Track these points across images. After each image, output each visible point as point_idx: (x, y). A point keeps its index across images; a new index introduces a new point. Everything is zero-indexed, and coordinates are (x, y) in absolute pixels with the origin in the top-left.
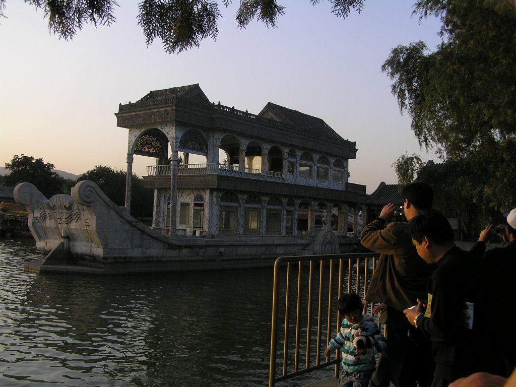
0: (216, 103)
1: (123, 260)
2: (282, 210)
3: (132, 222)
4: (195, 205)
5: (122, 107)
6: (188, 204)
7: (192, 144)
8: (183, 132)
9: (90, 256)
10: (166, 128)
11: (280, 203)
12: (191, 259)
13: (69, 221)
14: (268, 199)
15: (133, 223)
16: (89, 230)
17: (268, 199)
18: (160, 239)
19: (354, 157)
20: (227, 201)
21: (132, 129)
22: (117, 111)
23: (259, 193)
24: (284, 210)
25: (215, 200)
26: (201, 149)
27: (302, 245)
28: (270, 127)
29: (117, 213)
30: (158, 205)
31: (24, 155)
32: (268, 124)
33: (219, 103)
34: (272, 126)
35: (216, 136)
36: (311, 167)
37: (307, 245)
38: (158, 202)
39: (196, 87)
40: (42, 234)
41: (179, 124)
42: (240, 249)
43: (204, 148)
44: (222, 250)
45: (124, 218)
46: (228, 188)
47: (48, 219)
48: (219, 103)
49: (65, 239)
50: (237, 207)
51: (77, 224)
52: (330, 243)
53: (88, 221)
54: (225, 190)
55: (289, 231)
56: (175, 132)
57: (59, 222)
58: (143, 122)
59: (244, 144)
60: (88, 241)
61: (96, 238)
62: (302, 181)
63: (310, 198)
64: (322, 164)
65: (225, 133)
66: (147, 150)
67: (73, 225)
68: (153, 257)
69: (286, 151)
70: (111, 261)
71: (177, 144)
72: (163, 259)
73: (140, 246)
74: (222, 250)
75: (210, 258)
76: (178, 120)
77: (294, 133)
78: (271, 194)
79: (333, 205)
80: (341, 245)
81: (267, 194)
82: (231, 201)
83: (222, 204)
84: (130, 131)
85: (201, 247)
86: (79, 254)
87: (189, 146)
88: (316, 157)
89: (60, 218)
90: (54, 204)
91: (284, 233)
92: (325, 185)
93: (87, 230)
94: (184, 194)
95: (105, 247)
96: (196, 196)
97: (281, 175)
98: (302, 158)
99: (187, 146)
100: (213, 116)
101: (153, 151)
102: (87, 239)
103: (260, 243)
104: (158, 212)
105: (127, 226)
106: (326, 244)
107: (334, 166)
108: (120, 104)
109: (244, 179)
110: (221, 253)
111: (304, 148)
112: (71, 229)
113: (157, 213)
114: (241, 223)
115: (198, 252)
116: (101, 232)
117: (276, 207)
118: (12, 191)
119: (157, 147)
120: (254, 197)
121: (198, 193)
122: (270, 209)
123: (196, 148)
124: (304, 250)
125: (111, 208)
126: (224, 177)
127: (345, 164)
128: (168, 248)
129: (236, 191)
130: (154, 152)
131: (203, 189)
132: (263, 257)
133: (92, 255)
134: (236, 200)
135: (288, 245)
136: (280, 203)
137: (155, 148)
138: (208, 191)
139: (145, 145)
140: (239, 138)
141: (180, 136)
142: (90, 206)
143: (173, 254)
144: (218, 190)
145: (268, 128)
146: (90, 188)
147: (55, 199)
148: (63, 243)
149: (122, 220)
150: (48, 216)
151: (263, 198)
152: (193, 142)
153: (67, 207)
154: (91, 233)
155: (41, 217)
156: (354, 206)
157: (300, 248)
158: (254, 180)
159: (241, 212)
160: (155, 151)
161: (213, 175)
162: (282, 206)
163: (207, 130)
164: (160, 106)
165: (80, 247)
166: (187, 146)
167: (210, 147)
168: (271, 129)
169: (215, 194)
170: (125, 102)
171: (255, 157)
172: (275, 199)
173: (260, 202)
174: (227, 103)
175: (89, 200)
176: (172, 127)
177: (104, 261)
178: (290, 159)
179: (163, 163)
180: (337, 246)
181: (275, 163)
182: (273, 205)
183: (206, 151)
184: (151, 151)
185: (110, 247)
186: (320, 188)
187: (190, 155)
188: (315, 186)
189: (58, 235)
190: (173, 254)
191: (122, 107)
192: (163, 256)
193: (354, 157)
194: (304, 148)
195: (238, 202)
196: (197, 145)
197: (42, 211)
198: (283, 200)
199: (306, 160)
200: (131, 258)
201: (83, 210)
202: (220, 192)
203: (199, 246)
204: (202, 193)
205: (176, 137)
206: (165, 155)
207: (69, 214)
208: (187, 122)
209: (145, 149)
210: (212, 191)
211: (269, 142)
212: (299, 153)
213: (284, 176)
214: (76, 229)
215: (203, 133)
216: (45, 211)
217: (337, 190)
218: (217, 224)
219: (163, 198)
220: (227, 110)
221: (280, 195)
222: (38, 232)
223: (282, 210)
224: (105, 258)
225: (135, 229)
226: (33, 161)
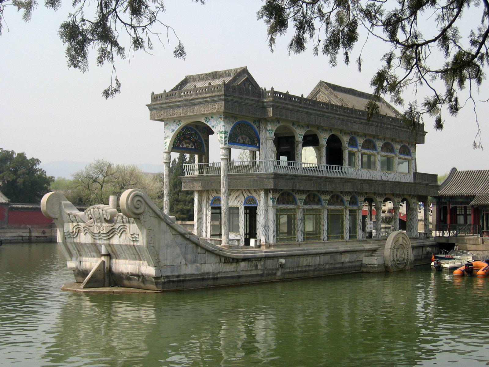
0: (268, 89)
1: (177, 279)
3: (186, 234)
4: (246, 208)
5: (155, 98)
6: (238, 208)
7: (242, 138)
8: (232, 125)
9: (138, 276)
10: (212, 120)
11: (342, 202)
12: (249, 273)
13: (111, 236)
14: (328, 197)
15: (186, 235)
16: (138, 246)
17: (328, 197)
18: (216, 252)
19: (423, 142)
20: (284, 203)
21: (168, 122)
22: (149, 102)
23: (318, 192)
24: (346, 209)
25: (270, 202)
26: (253, 142)
27: (368, 251)
28: (328, 113)
29: (168, 224)
30: (200, 211)
31: (4, 150)
32: (325, 110)
33: (272, 89)
34: (330, 110)
35: (269, 127)
36: (369, 156)
37: (374, 250)
38: (200, 206)
39: (245, 71)
40: (74, 252)
41: (227, 116)
43: (256, 142)
44: (283, 261)
45: (175, 230)
46: (286, 188)
47: (82, 234)
48: (272, 89)
49: (106, 257)
50: (294, 209)
52: (402, 246)
53: (135, 235)
54: (281, 190)
55: (353, 236)
56: (224, 126)
57: (97, 238)
58: (183, 115)
59: (299, 134)
60: (135, 259)
61: (147, 254)
62: (365, 174)
63: (375, 194)
64: (387, 152)
65: (279, 123)
66: (185, 146)
67: (116, 241)
68: (208, 273)
69: (345, 140)
70: (163, 281)
71: (226, 139)
72: (219, 276)
73: (194, 262)
74: (283, 261)
75: (270, 272)
76: (227, 111)
77: (355, 118)
78: (332, 192)
79: (400, 200)
80: (413, 248)
81: (326, 193)
82: (288, 204)
83: (280, 206)
84: (166, 124)
85: (259, 259)
86: (123, 274)
87: (239, 140)
88: (379, 144)
89: (99, 233)
90: (90, 216)
91: (348, 237)
92: (390, 177)
93: (134, 245)
94: (231, 197)
95: (158, 265)
96: (247, 198)
97: (342, 169)
98: (363, 147)
99: (237, 141)
100: (265, 104)
101: (192, 146)
102: (134, 256)
103: (324, 251)
104: (200, 219)
105: (179, 239)
106: (398, 249)
107: (401, 153)
108: (153, 93)
109: (302, 176)
110: (282, 266)
111: (365, 135)
112: (113, 245)
113: (198, 219)
115: (256, 266)
116: (153, 248)
117: (338, 207)
118: (39, 203)
119: (196, 142)
120: (312, 198)
121: (250, 195)
123: (246, 142)
124: (372, 256)
125: (162, 220)
126: (281, 175)
127: (412, 150)
128: (225, 263)
129: (293, 191)
130: (193, 147)
131: (255, 190)
132: (327, 267)
133: (140, 274)
134: (294, 202)
136: (342, 202)
137: (194, 143)
138: (262, 194)
139: (183, 140)
140: (294, 128)
141: (229, 129)
142: (139, 219)
143: (229, 268)
144: (275, 191)
145: (327, 114)
146: (137, 199)
147: (92, 210)
148: (103, 262)
149: (174, 233)
150: (82, 230)
151: (323, 197)
152: (243, 136)
153: (109, 218)
154: (139, 249)
155: (73, 232)
156: (423, 199)
157: (367, 254)
158: (313, 177)
160: (195, 147)
161: (270, 174)
162: (344, 205)
163: (259, 121)
164: (204, 95)
165: (123, 266)
166: (237, 141)
167: (262, 140)
168: (329, 115)
169: (271, 195)
170: (159, 91)
171: (304, 148)
172: (336, 198)
173: (319, 202)
174: (281, 88)
175: (138, 212)
176: (220, 120)
177: (156, 281)
178: (351, 149)
179: (203, 161)
180: (410, 250)
181: (334, 156)
182: (333, 204)
183: (258, 145)
184: (190, 147)
185: (162, 265)
186: (386, 181)
187: (233, 150)
188: (379, 179)
189: (96, 252)
190: (229, 268)
191: (155, 98)
192: (219, 272)
193: (423, 142)
194: (365, 135)
195: (296, 204)
196: (248, 139)
197: (75, 224)
199: (368, 149)
200: (185, 275)
201: (129, 222)
202: (276, 193)
203: (258, 258)
204: (254, 195)
205: (225, 131)
206: (206, 151)
207: (111, 228)
208: (237, 113)
209: (183, 145)
210: (267, 191)
211: (326, 130)
212: (360, 141)
213: (346, 170)
214: (120, 245)
215: (253, 124)
216: (78, 225)
217: (405, 183)
218: (274, 231)
219: (205, 202)
220: (281, 96)
221: (341, 192)
222: (69, 249)
224: (156, 278)
225: (188, 242)
226: (15, 156)
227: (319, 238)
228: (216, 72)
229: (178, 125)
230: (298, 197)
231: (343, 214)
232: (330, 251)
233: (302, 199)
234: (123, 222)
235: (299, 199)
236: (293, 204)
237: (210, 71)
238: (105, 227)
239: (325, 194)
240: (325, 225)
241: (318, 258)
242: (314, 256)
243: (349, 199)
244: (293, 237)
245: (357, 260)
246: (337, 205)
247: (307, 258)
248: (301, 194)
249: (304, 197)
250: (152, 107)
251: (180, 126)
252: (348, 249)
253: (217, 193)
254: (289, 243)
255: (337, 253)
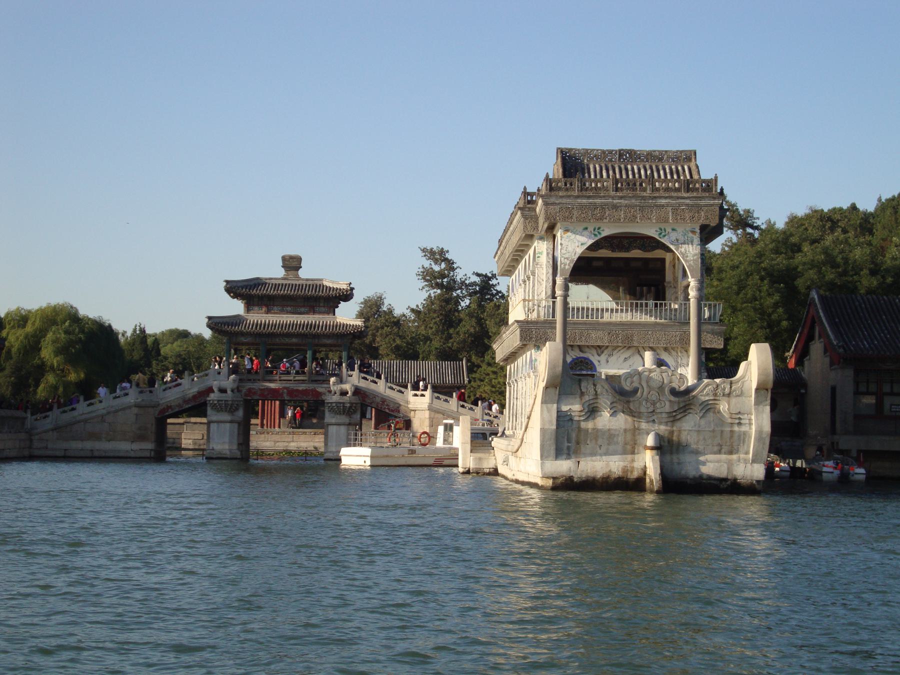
13: (679, 417)
47: (606, 414)
51: (703, 422)
94: (612, 359)
131: (666, 349)
176: (690, 235)
228: (631, 153)
229: (595, 235)
234: (715, 395)
237: (616, 147)
238: (667, 403)
250: (552, 200)
251: (599, 237)
253: (581, 351)
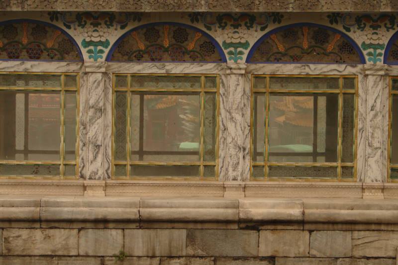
2: (360, 77)
14: (253, 37)
17: (253, 37)
42: (25, 233)
50: (71, 78)
78: (276, 17)
81: (247, 19)
82: (35, 56)
114: (91, 134)
122: (274, 78)
134: (67, 50)
135: (331, 224)
151: (220, 37)
159: (94, 91)
173: (210, 50)
182: (295, 59)
198: (359, 37)
223: (360, 77)
227: (210, 170)
230: (79, 36)
231: (356, 94)
232: (176, 216)
233: (105, 44)
235: (86, 44)
236: (62, 59)
239: (236, 26)
240: (231, 126)
241: (115, 235)
242: (88, 225)
243: (385, 41)
244: (61, 162)
245: (358, 253)
246: (319, 62)
247: (52, 232)
248: (96, 25)
249: (113, 36)
252: (295, 212)
254: (38, 179)
255: (227, 222)
